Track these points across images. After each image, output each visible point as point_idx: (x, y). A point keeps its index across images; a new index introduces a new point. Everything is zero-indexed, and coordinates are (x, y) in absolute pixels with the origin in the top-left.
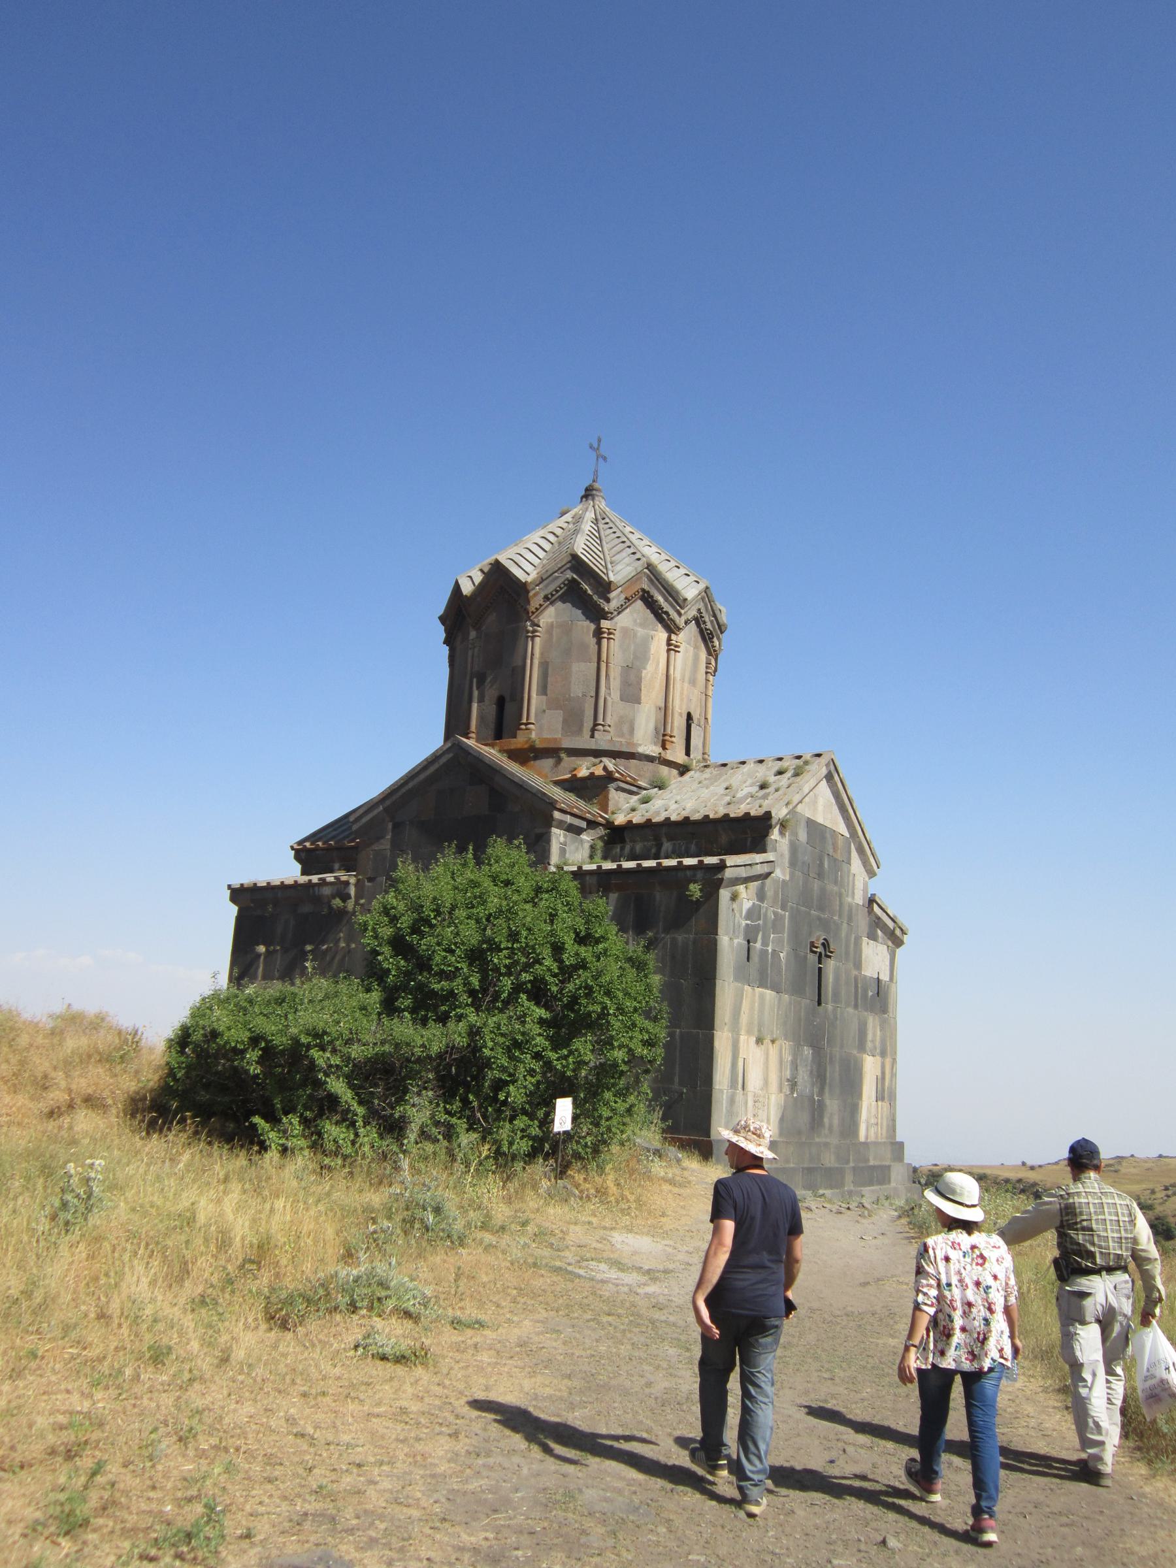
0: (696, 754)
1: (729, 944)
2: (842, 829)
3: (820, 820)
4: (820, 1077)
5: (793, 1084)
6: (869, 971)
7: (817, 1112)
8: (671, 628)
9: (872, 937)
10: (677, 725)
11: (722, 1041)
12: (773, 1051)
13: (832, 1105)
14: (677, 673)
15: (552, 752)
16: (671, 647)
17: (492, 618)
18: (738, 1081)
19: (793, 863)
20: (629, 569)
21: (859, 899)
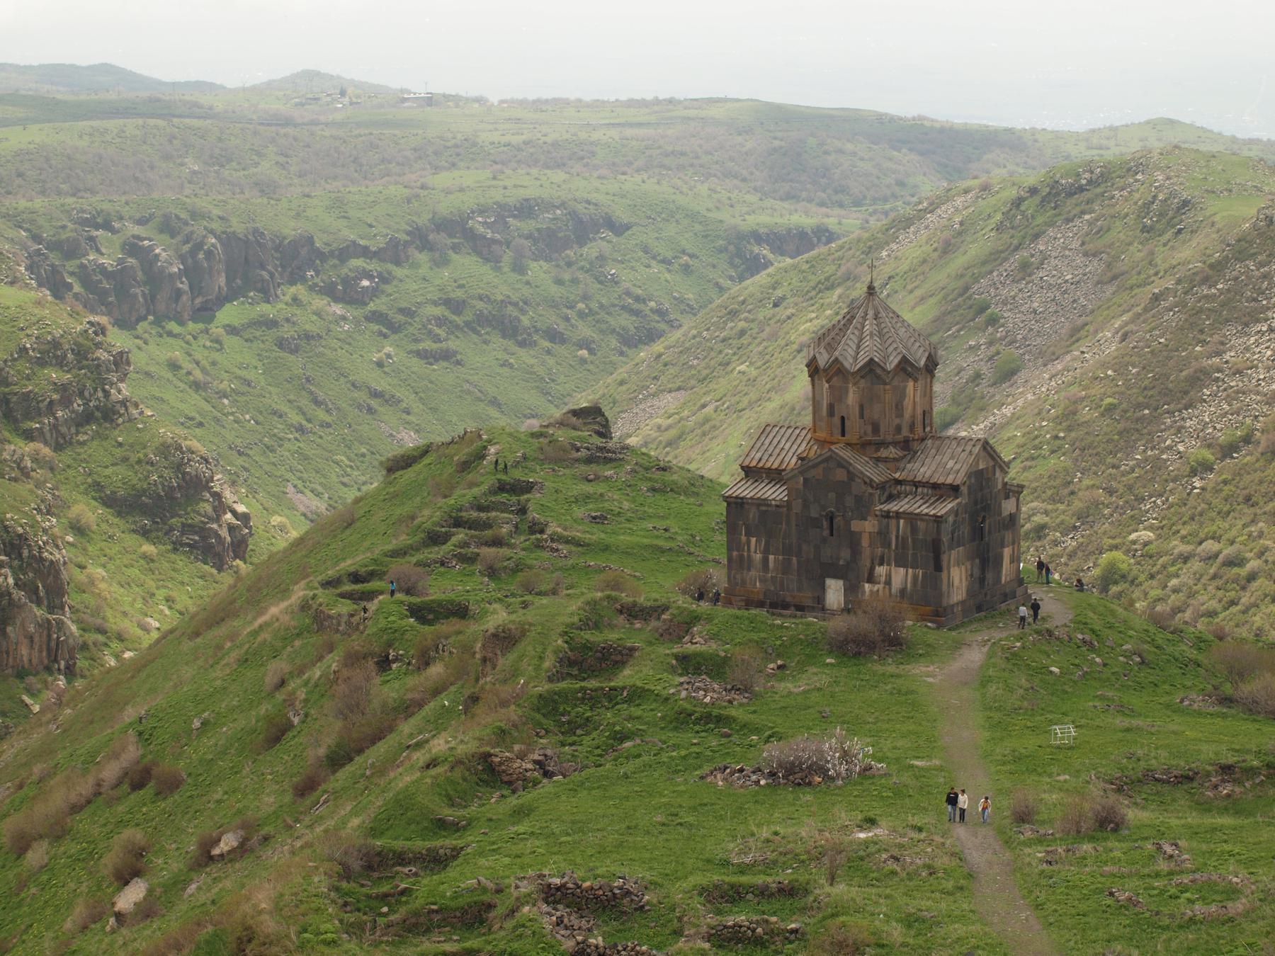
0: (928, 429)
1: (945, 539)
2: (992, 463)
3: (981, 467)
4: (983, 570)
5: (972, 575)
6: (1005, 513)
7: (982, 580)
8: (916, 380)
9: (1007, 497)
10: (920, 417)
11: (944, 575)
12: (963, 568)
13: (990, 576)
14: (918, 399)
15: (869, 443)
16: (915, 390)
17: (835, 379)
18: (950, 584)
19: (969, 493)
20: (896, 361)
21: (1000, 486)
